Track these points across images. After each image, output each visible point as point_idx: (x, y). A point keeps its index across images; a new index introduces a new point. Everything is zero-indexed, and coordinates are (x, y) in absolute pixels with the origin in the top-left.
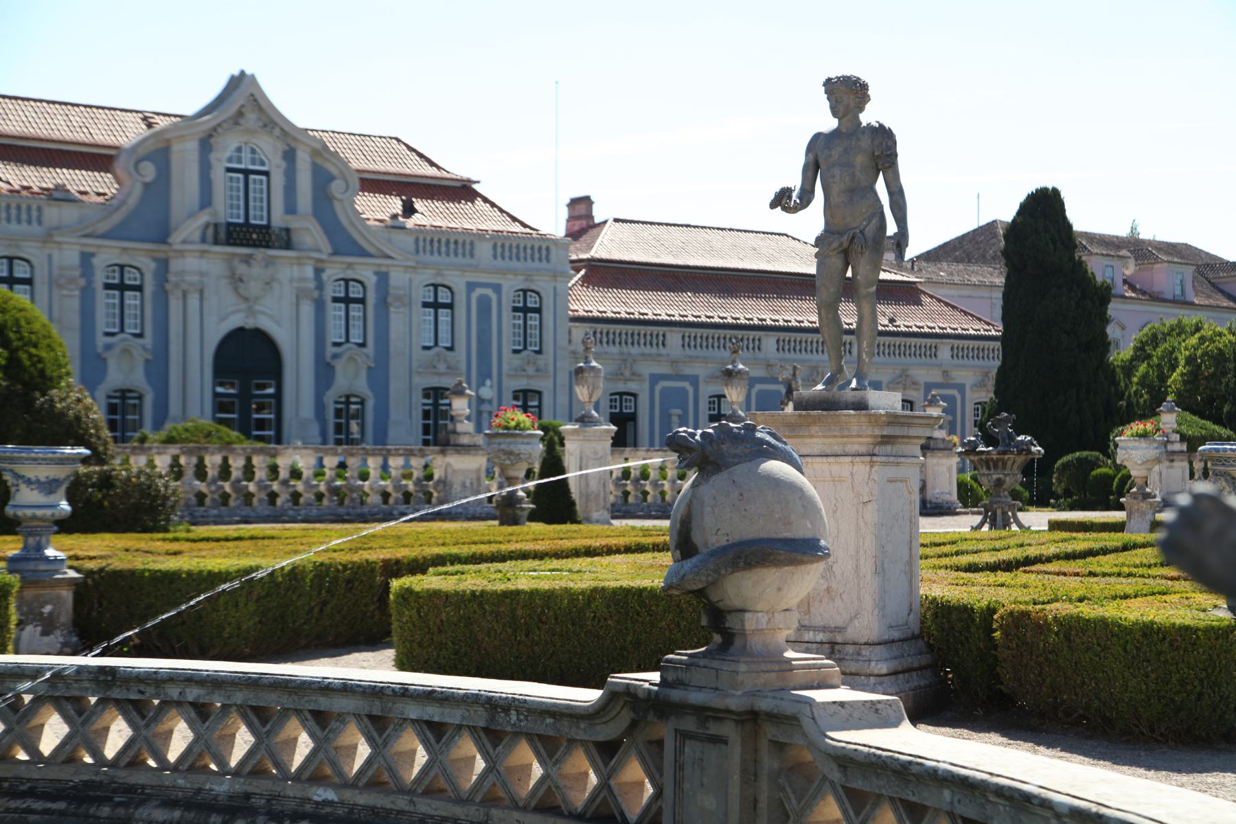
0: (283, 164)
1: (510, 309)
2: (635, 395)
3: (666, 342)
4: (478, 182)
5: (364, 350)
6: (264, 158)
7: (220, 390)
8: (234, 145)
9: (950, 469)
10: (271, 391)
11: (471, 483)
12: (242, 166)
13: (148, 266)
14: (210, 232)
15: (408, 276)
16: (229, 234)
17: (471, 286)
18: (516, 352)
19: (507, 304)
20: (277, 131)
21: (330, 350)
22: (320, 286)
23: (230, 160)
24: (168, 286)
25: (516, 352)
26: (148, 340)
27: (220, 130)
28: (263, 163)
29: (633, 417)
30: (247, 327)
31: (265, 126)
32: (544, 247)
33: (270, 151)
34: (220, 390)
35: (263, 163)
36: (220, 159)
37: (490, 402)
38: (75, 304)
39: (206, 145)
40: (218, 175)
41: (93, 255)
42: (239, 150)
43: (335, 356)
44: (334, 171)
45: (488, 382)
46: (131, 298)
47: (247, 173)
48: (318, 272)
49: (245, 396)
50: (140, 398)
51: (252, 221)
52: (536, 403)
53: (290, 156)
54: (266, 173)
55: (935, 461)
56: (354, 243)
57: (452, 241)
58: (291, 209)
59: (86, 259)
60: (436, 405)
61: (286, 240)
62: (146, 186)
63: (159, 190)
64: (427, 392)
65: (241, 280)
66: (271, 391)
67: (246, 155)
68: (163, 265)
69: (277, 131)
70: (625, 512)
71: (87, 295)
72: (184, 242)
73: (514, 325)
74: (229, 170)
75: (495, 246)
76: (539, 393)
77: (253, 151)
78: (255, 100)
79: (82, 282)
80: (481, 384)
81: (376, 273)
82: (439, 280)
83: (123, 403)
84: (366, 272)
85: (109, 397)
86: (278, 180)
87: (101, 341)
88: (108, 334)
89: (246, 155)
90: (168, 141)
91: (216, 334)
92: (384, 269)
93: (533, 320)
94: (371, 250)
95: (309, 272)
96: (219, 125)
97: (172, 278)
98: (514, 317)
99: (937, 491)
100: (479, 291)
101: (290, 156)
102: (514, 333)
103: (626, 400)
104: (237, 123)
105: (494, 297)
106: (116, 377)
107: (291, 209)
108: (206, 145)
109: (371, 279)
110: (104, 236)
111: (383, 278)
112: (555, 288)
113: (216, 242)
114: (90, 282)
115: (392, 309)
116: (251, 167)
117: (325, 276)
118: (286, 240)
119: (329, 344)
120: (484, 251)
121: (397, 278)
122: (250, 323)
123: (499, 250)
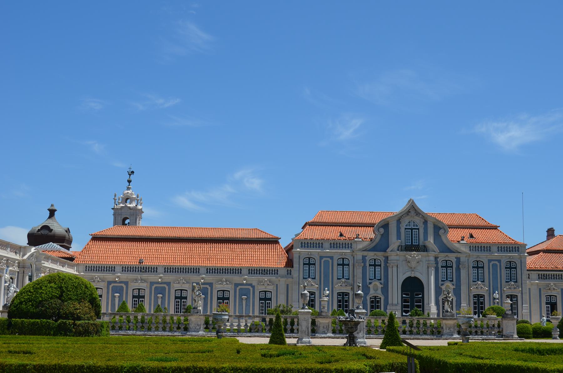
1: (505, 268)
2: (556, 296)
3: (530, 277)
4: (499, 227)
5: (452, 283)
6: (417, 224)
7: (404, 296)
8: (407, 223)
9: (513, 324)
10: (421, 296)
11: (326, 327)
12: (411, 227)
13: (383, 259)
14: (400, 247)
16: (406, 248)
17: (490, 261)
18: (506, 282)
19: (503, 265)
20: (421, 216)
21: (440, 283)
22: (437, 263)
23: (406, 226)
24: (388, 265)
25: (506, 282)
26: (382, 281)
27: (403, 217)
28: (417, 226)
29: (555, 304)
30: (412, 276)
31: (417, 215)
32: (517, 247)
33: (418, 221)
34: (404, 296)
35: (417, 226)
36: (403, 226)
37: (498, 299)
38: (361, 271)
39: (399, 221)
40: (403, 231)
41: (366, 256)
42: (409, 222)
43: (442, 285)
44: (441, 227)
46: (378, 269)
47: (412, 229)
48: (436, 258)
49: (412, 298)
50: (380, 298)
52: (516, 299)
53: (425, 222)
54: (418, 229)
55: (507, 321)
56: (448, 248)
57: (483, 246)
59: (364, 257)
60: (478, 300)
61: (425, 249)
62: (382, 235)
63: (385, 237)
64: (475, 296)
65: (409, 262)
66: (421, 296)
67: (412, 224)
68: (387, 258)
69: (421, 216)
70: (499, 337)
71: (364, 268)
72: (391, 251)
73: (507, 273)
74: (406, 229)
75: (498, 247)
76: (517, 296)
77: (414, 222)
78: (414, 207)
79: (363, 264)
80: (494, 292)
81: (456, 258)
83: (375, 300)
84: (452, 257)
85: (370, 298)
86: (422, 231)
87: (368, 281)
88: (370, 279)
89: (412, 224)
90: (388, 221)
91: (402, 278)
92: (458, 256)
93: (480, 271)
94: (454, 251)
95: (432, 259)
96: (402, 215)
97: (389, 262)
98: (506, 270)
99: (508, 332)
100: (492, 262)
101: (425, 222)
102: (507, 276)
103: (553, 298)
104: (408, 215)
105: (498, 264)
106: (372, 293)
108: (399, 221)
109: (454, 260)
110: (369, 251)
111: (458, 259)
112: (521, 260)
113: (401, 251)
114: (365, 265)
116: (413, 227)
117: (438, 259)
118: (425, 249)
119: (440, 280)
120: (494, 249)
121: (463, 259)
122: (413, 276)
123: (500, 249)
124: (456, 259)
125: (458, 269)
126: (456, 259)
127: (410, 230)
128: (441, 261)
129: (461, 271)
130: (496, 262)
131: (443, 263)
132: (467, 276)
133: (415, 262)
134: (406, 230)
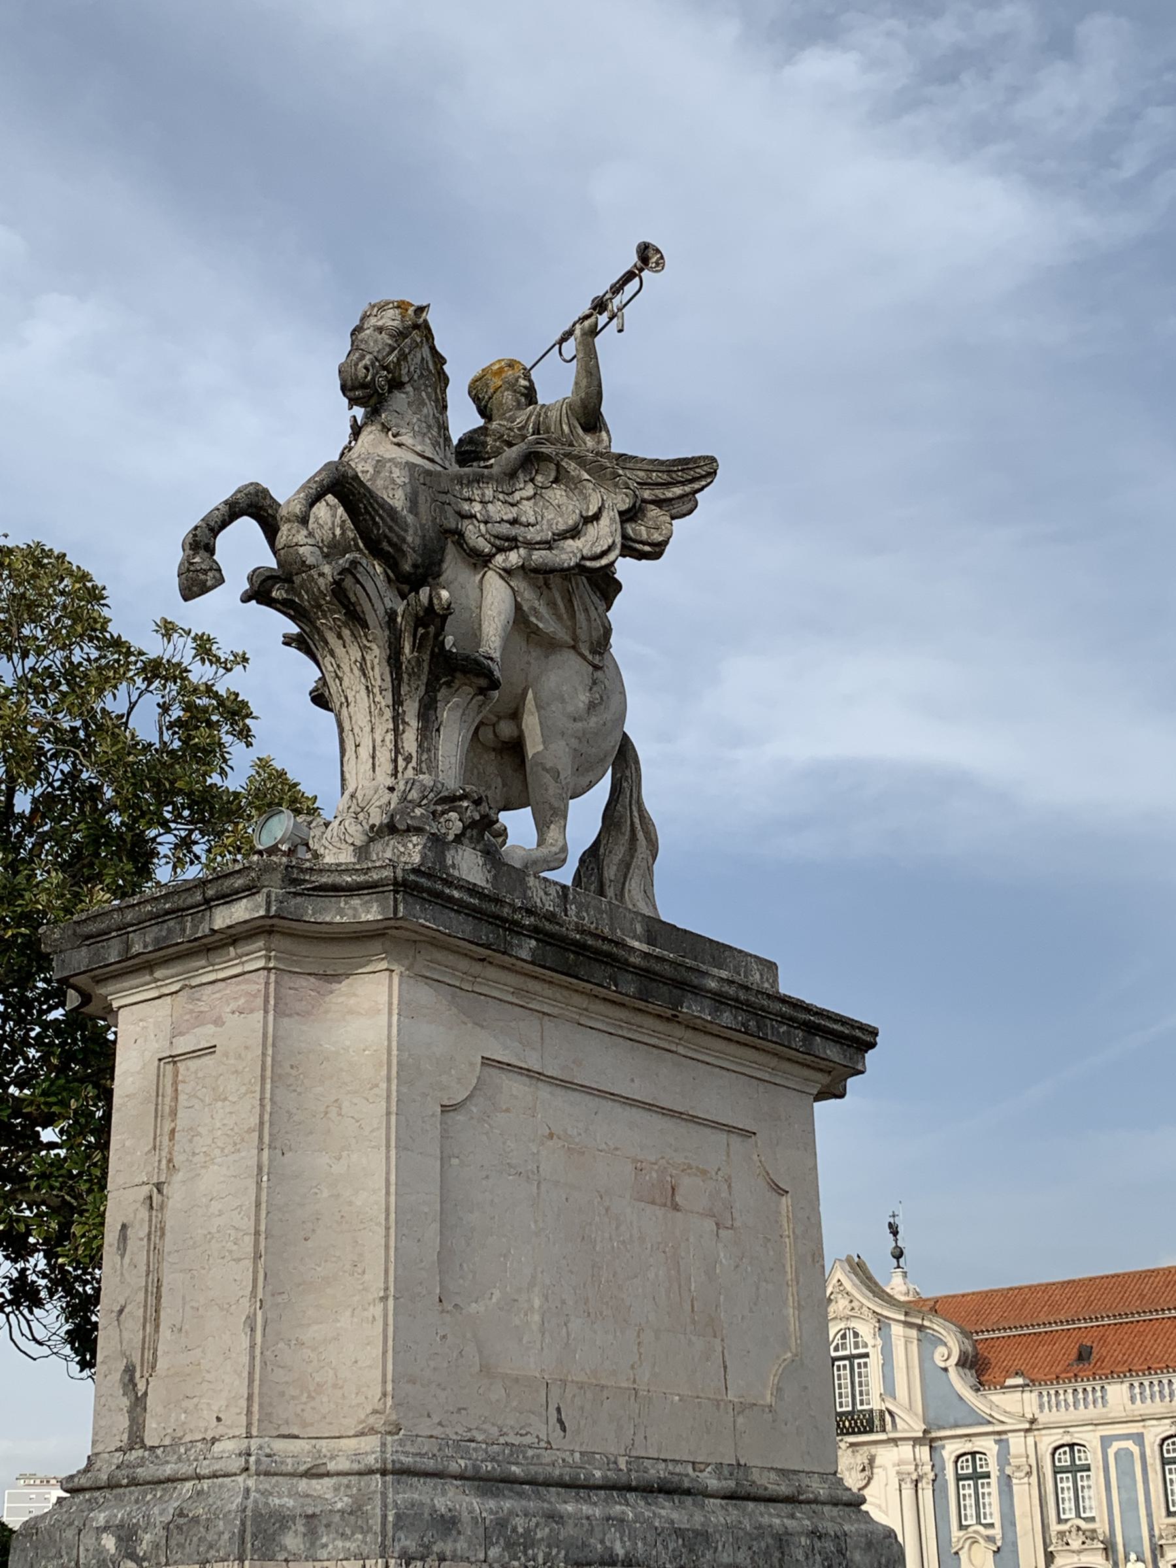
0: (879, 1342)
12: (847, 1353)
15: (1030, 1440)
17: (1106, 1441)
28: (866, 1346)
45: (1133, 1557)
47: (850, 1358)
51: (859, 1408)
54: (866, 1355)
58: (889, 1390)
77: (856, 1335)
81: (996, 1442)
82: (1067, 1439)
100: (1116, 1445)
105: (1136, 1450)
107: (889, 1390)
115: (1014, 1481)
116: (855, 1352)
124: (996, 1447)
125: (1006, 1482)
126: (996, 1447)
127: (847, 1362)
128: (953, 1458)
129: (1015, 1488)
130: (1129, 1444)
131: (965, 1464)
132: (1036, 1502)
133: (853, 1472)
134: (837, 1363)
